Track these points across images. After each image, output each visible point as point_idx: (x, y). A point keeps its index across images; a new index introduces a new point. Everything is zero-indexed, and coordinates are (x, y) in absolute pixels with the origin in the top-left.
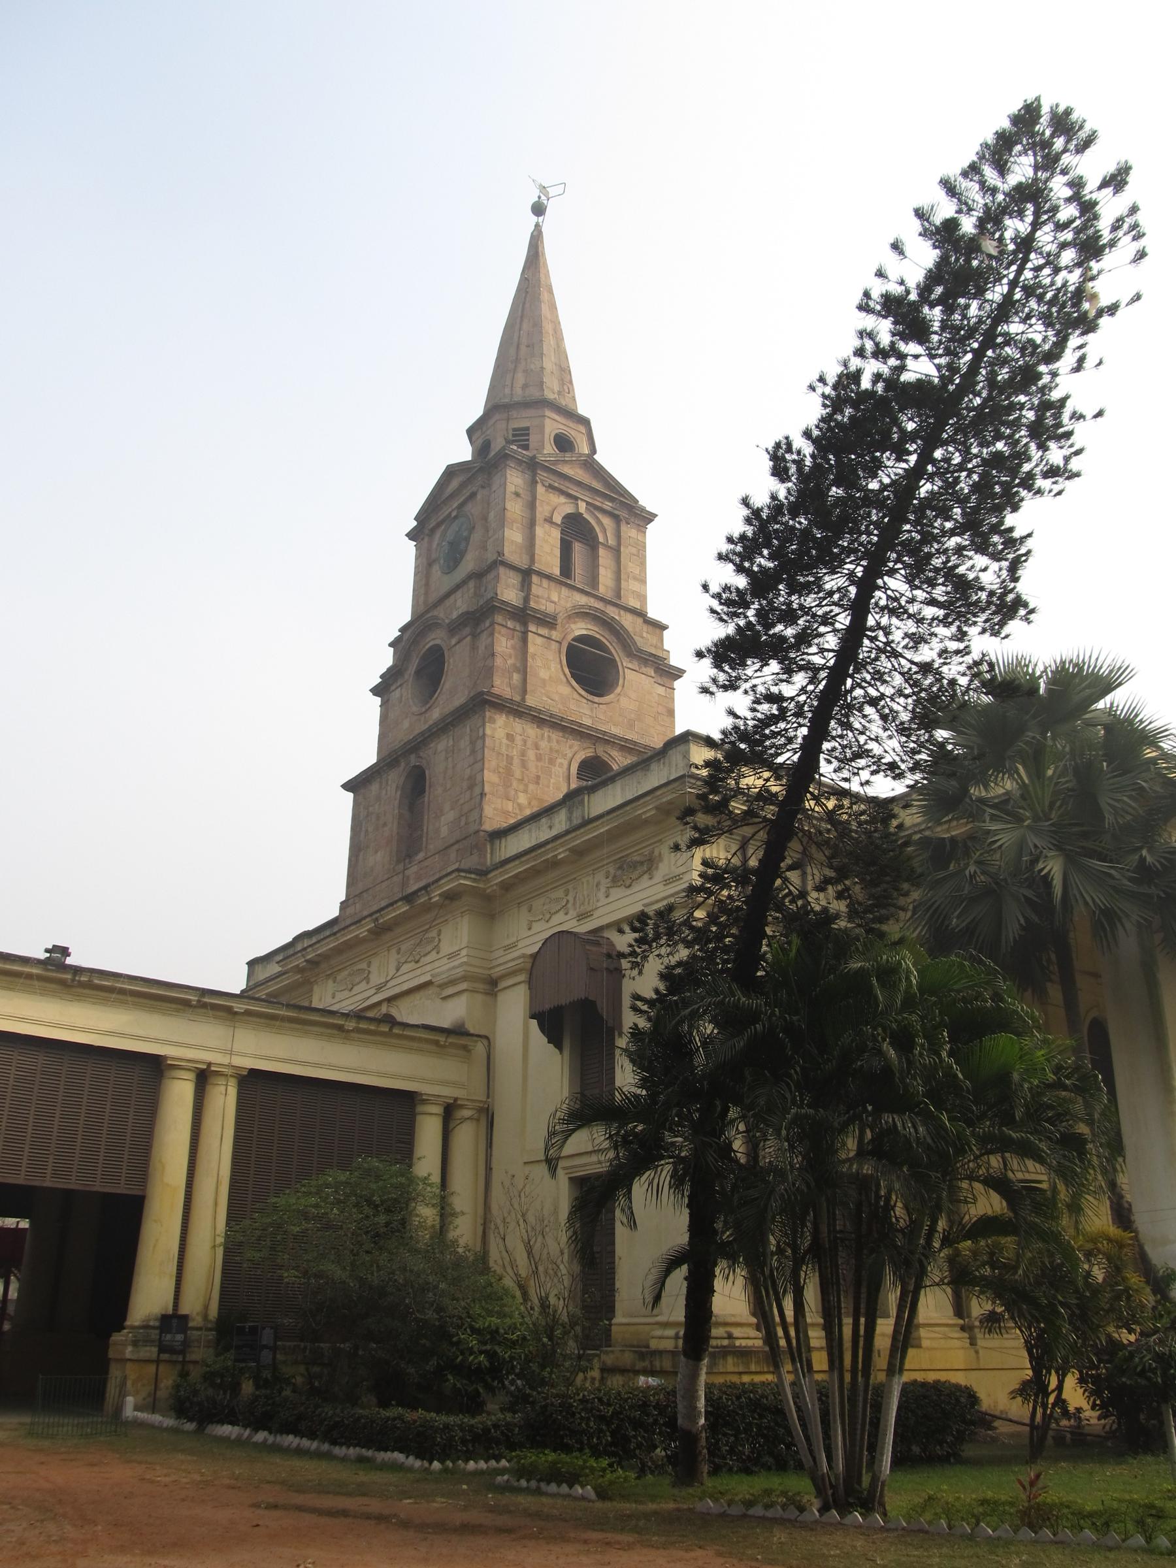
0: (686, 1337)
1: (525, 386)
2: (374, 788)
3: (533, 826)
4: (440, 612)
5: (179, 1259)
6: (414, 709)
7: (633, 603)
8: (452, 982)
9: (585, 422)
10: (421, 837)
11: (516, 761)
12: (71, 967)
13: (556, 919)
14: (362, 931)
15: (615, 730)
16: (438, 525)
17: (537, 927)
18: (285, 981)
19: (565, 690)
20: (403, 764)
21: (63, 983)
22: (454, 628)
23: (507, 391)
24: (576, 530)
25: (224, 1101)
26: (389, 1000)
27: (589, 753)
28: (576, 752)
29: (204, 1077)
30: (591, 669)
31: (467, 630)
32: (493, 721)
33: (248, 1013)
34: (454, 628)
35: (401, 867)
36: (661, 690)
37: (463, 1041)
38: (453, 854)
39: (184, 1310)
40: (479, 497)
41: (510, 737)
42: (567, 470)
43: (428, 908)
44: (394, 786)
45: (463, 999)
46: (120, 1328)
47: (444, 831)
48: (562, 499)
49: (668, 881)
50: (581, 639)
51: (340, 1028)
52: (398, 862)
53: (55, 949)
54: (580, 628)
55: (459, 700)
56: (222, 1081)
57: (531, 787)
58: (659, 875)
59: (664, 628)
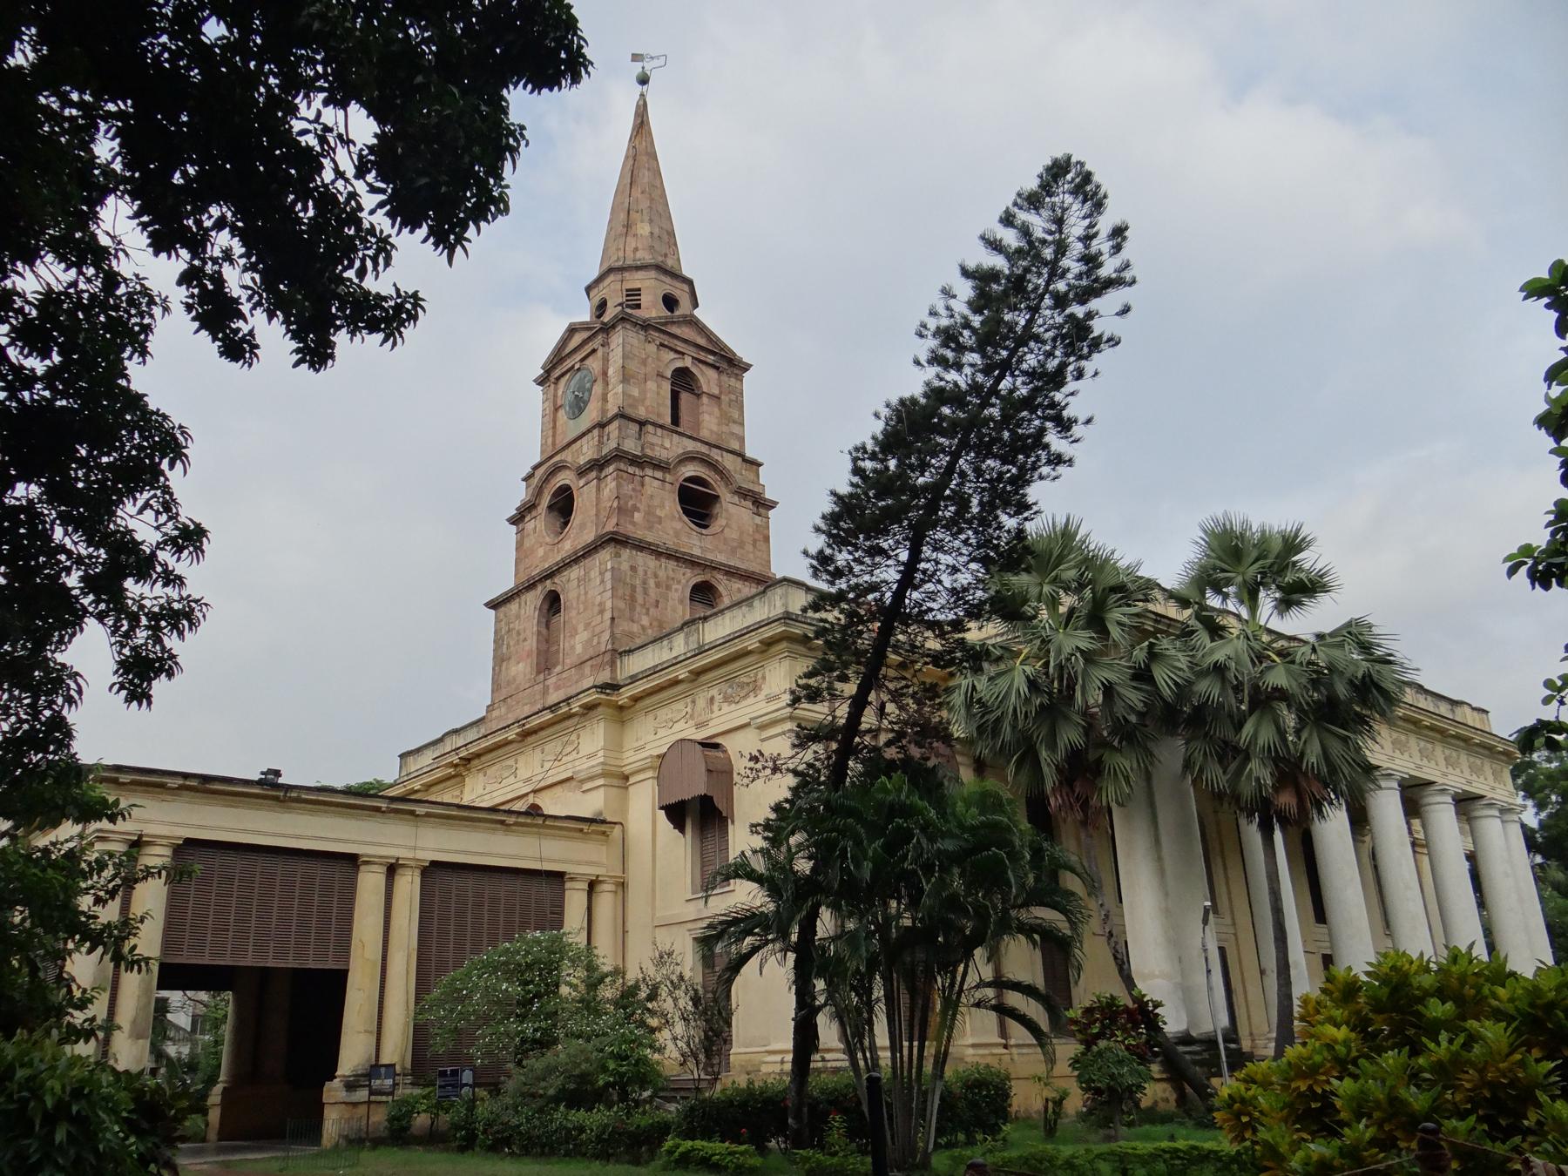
0: (794, 1061)
1: (636, 249)
2: (513, 607)
3: (657, 646)
4: (567, 456)
5: (378, 1021)
6: (548, 539)
7: (735, 446)
8: (591, 778)
9: (690, 283)
10: (558, 651)
11: (639, 590)
12: (283, 786)
13: (677, 727)
14: (511, 734)
15: (721, 558)
16: (563, 375)
17: (661, 733)
18: (439, 774)
19: (679, 525)
20: (540, 588)
21: (276, 798)
22: (582, 472)
23: (621, 254)
24: (683, 381)
25: (408, 886)
26: (535, 791)
27: (699, 579)
28: (690, 578)
29: (392, 870)
30: (697, 504)
31: (593, 474)
32: (618, 555)
33: (428, 815)
34: (582, 472)
35: (542, 676)
36: (758, 520)
37: (603, 828)
38: (587, 668)
39: (385, 1059)
40: (600, 353)
41: (633, 569)
42: (675, 330)
43: (569, 716)
45: (602, 790)
46: (332, 1077)
47: (579, 649)
48: (672, 355)
49: (770, 699)
50: (690, 479)
51: (502, 822)
52: (538, 673)
53: (270, 771)
54: (690, 470)
55: (589, 536)
56: (409, 872)
57: (652, 610)
58: (762, 696)
59: (760, 465)
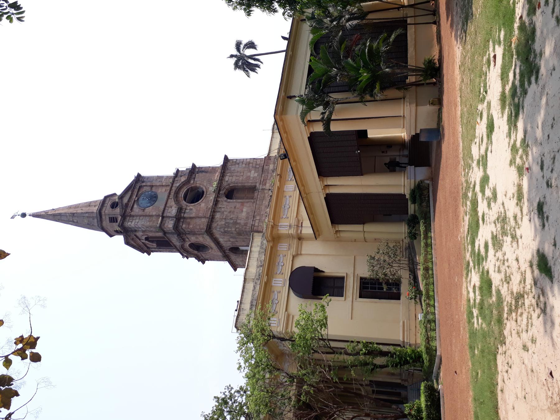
20: (219, 199)
38: (266, 167)
44: (225, 203)
